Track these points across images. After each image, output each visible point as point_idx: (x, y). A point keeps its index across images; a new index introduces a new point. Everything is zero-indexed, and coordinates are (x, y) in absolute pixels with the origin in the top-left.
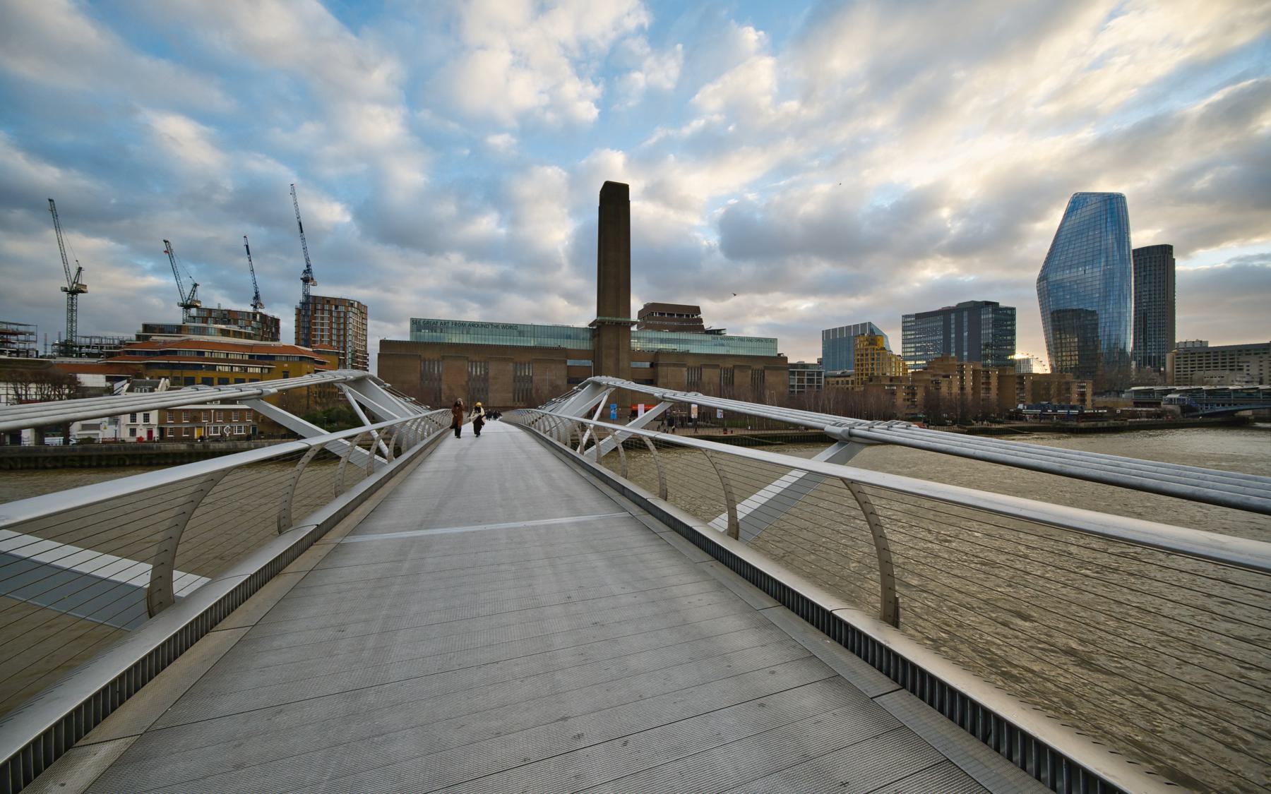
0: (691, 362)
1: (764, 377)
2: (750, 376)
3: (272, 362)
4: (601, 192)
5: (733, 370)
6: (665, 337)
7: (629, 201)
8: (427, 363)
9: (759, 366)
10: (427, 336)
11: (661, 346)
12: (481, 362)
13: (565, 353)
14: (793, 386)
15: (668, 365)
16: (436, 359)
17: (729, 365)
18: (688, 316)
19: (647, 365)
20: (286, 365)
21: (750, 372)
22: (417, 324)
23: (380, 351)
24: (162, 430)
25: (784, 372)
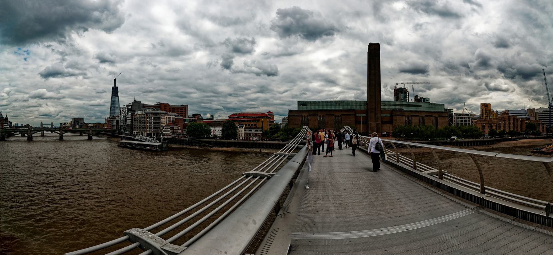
0: (407, 114)
2: (432, 120)
6: (396, 103)
8: (304, 117)
9: (436, 115)
10: (303, 108)
11: (394, 107)
12: (322, 116)
13: (355, 111)
14: (458, 123)
17: (423, 115)
19: (389, 115)
20: (262, 119)
21: (432, 118)
22: (300, 104)
24: (244, 138)
25: (446, 118)
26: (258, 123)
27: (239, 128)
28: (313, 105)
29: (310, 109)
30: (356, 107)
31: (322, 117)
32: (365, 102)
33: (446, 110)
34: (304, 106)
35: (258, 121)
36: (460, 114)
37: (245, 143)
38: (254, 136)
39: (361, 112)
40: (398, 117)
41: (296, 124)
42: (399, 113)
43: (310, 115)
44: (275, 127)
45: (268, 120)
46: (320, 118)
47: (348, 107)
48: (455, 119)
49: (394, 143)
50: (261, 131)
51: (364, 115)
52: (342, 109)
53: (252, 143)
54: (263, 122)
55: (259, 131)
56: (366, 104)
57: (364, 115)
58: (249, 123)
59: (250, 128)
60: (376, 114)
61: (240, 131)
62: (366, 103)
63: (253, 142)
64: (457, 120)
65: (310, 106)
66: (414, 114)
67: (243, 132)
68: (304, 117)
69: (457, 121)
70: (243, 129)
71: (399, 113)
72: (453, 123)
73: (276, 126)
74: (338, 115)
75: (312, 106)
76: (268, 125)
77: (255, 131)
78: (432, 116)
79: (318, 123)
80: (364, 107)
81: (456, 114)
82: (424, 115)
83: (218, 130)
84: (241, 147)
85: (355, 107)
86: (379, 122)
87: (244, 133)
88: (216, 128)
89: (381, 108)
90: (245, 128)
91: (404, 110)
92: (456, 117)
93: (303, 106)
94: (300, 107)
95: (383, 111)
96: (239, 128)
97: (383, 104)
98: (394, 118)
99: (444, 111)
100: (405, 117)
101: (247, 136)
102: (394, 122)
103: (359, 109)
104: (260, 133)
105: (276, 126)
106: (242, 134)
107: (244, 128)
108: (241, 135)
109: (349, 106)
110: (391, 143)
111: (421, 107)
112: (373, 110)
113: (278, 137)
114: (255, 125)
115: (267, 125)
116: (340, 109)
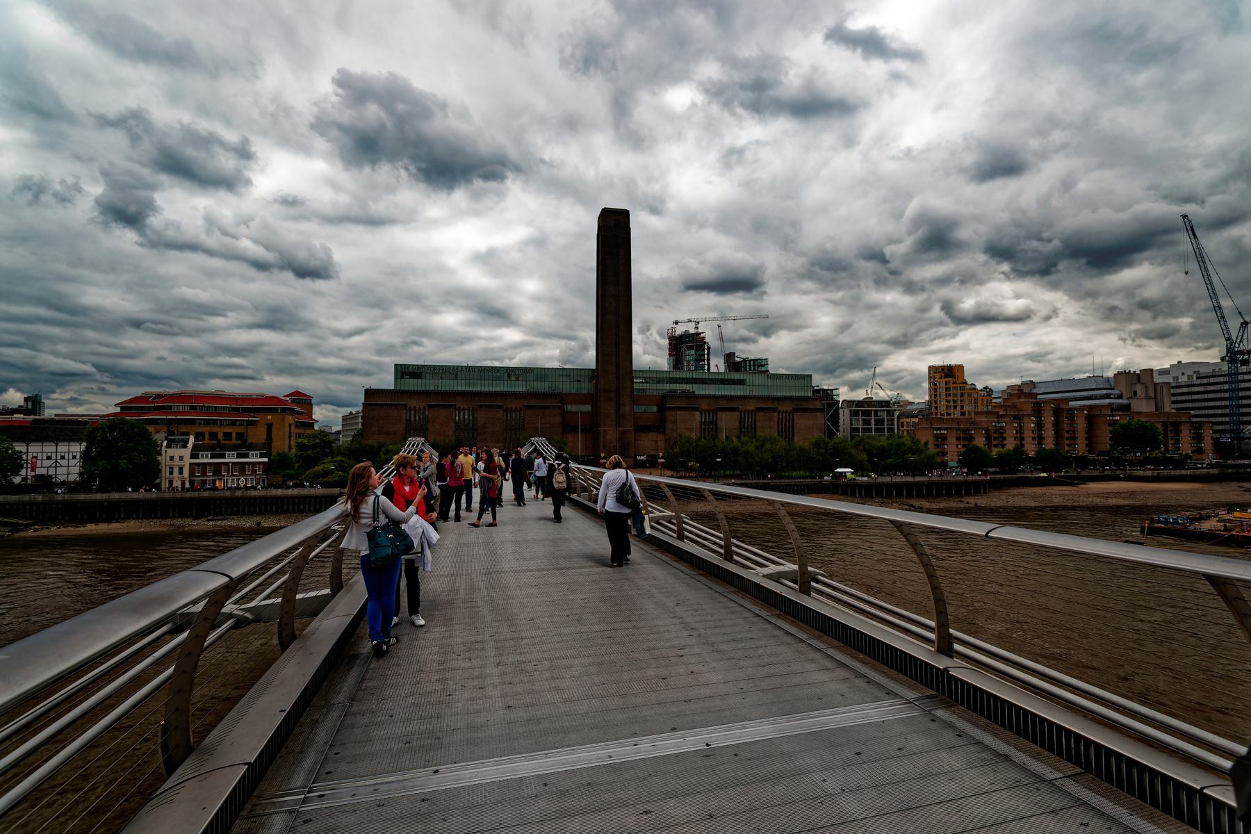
0: (704, 405)
4: (599, 218)
7: (630, 229)
8: (412, 412)
9: (787, 407)
10: (412, 384)
11: (669, 387)
12: (469, 409)
13: (562, 398)
14: (857, 430)
15: (673, 409)
16: (422, 408)
17: (751, 406)
19: (655, 409)
20: (269, 417)
21: (776, 414)
22: (403, 371)
24: (192, 482)
25: (818, 414)
26: (251, 431)
27: (168, 446)
28: (441, 378)
29: (432, 388)
30: (566, 387)
31: (466, 412)
32: (590, 372)
33: (818, 391)
34: (416, 380)
35: (252, 423)
36: (859, 401)
37: (192, 499)
38: (232, 475)
39: (579, 398)
40: (679, 412)
41: (388, 433)
42: (682, 403)
43: (431, 406)
44: (317, 441)
45: (290, 419)
46: (462, 414)
47: (543, 387)
48: (844, 416)
49: (669, 486)
50: (262, 456)
51: (587, 408)
53: (226, 499)
54: (269, 427)
55: (255, 458)
56: (593, 378)
57: (587, 408)
58: (215, 429)
59: (218, 448)
60: (618, 405)
61: (172, 458)
62: (593, 375)
63: (228, 494)
64: (851, 420)
65: (432, 381)
66: (722, 404)
67: (188, 460)
68: (412, 412)
69: (851, 424)
70: (186, 453)
71: (682, 403)
72: (841, 429)
73: (321, 439)
74: (514, 407)
75: (440, 381)
76: (290, 437)
77: (239, 456)
78: (775, 410)
79: (457, 430)
80: (586, 387)
81: (849, 402)
82: (754, 408)
83: (63, 458)
84: (174, 517)
85: (561, 386)
86: (629, 427)
87: (191, 464)
88: (50, 448)
89: (632, 389)
90: (195, 448)
91: (697, 393)
92: (847, 411)
93: (411, 380)
94: (403, 380)
95: (639, 398)
96: (168, 446)
97: (639, 378)
98: (670, 415)
99: (810, 394)
100: (698, 413)
101: (204, 474)
102: (669, 426)
103: (573, 391)
104: (259, 463)
105: (321, 439)
107: (190, 445)
108: (176, 471)
109: (547, 382)
110: (662, 486)
111: (744, 384)
112: (612, 395)
113: (327, 473)
114: (240, 436)
115: (287, 434)
116: (520, 390)
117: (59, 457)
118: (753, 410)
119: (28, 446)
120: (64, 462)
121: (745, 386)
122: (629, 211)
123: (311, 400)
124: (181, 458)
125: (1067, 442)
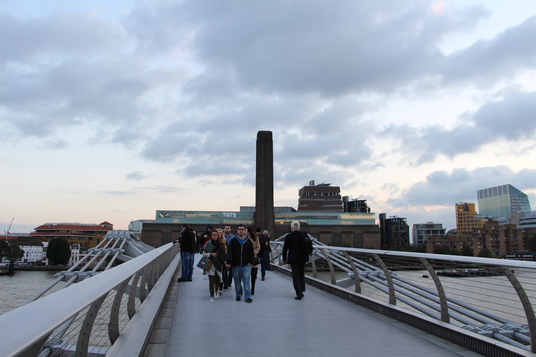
1: (362, 238)
3: (93, 234)
5: (341, 234)
9: (360, 231)
16: (169, 232)
17: (339, 231)
18: (331, 194)
20: (99, 236)
23: (143, 229)
52: (219, 223)
67: (79, 255)
70: (78, 251)
78: (352, 232)
83: (32, 252)
87: (80, 256)
106: (76, 258)
117: (31, 252)
118: (340, 233)
119: (23, 247)
120: (32, 254)
121: (337, 220)
122: (272, 132)
123: (112, 226)
124: (76, 254)
125: (513, 248)
